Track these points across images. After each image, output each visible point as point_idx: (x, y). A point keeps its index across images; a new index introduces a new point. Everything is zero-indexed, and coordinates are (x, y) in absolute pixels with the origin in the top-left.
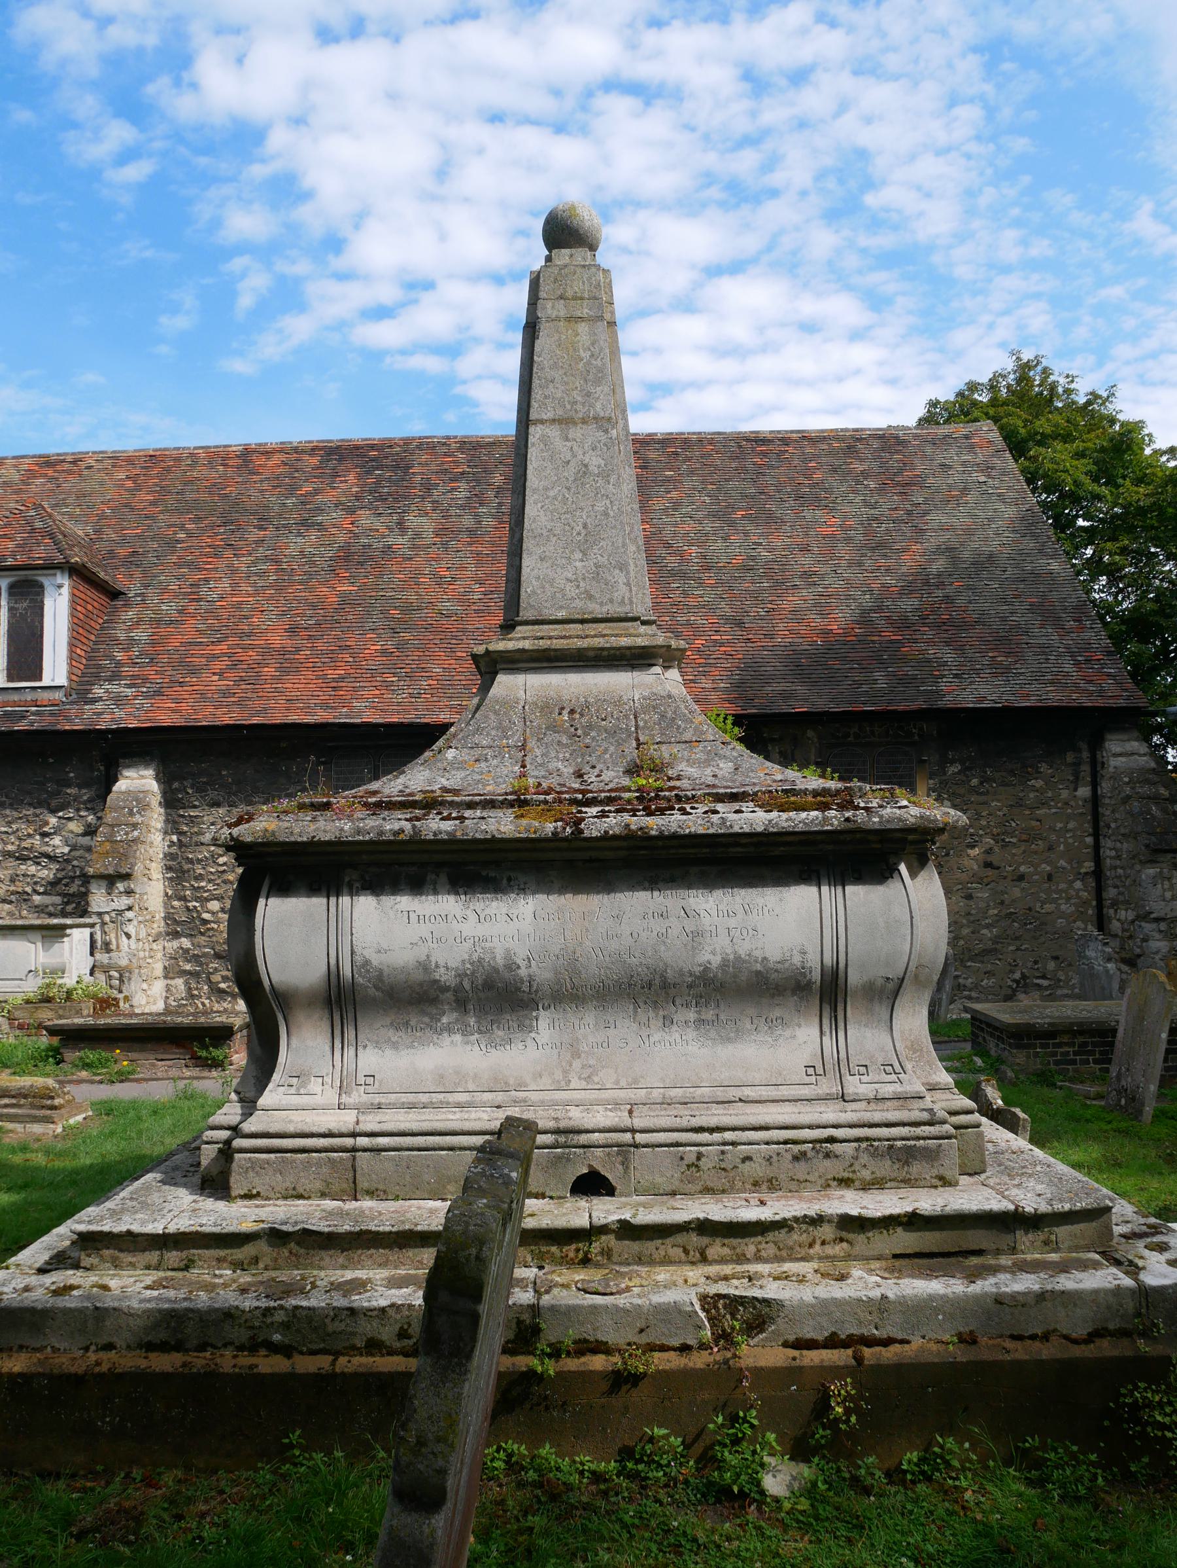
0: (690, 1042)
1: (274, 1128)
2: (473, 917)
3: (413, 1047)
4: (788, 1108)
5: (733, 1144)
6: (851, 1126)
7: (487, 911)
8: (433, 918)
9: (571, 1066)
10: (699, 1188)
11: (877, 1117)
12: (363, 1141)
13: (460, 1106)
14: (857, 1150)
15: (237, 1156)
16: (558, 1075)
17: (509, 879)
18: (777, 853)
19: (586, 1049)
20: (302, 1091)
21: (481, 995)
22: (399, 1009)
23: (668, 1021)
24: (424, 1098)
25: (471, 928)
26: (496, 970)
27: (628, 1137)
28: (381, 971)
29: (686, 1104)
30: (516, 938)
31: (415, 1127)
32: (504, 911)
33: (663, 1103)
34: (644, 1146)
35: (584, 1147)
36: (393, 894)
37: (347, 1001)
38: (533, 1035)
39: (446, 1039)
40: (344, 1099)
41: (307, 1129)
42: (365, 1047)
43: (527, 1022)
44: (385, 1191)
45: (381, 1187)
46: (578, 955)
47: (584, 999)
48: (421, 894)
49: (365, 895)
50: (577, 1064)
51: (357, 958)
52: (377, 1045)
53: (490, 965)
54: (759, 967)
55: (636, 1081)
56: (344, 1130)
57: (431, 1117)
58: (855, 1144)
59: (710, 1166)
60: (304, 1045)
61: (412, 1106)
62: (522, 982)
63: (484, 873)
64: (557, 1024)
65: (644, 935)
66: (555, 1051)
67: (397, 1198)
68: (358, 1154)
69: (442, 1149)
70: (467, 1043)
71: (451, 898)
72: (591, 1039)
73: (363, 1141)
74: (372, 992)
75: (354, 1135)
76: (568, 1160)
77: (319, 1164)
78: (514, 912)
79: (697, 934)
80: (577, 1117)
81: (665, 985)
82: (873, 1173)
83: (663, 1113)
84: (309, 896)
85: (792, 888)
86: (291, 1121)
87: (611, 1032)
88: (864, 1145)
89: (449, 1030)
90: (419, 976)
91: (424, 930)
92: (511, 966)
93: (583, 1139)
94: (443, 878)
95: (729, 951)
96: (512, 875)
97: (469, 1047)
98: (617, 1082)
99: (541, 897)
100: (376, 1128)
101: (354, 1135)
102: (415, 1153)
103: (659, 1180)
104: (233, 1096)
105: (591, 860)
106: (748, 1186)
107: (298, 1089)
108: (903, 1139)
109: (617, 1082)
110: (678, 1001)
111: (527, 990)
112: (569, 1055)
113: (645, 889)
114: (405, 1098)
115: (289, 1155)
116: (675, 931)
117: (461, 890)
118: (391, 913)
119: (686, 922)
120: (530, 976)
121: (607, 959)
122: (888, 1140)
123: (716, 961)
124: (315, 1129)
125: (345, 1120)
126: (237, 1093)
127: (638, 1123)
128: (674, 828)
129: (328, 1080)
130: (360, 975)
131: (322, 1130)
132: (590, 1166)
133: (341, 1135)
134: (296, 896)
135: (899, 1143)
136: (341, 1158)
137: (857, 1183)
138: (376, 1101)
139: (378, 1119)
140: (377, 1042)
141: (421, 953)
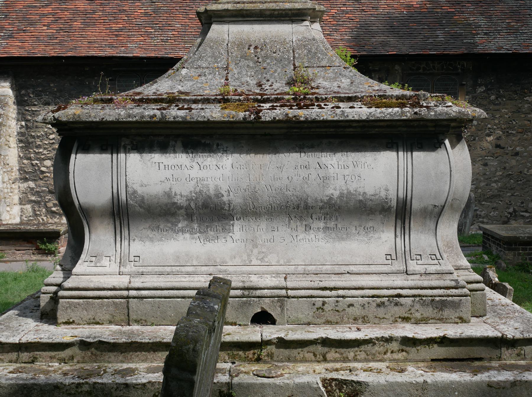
0: (320, 240)
1: (81, 285)
2: (196, 167)
3: (161, 240)
4: (375, 277)
5: (343, 297)
6: (411, 288)
7: (205, 163)
8: (173, 167)
9: (252, 252)
10: (323, 321)
11: (426, 284)
12: (133, 293)
13: (189, 274)
14: (413, 301)
15: (61, 300)
16: (245, 257)
17: (218, 145)
18: (373, 132)
19: (261, 243)
20: (98, 265)
21: (201, 211)
22: (154, 219)
23: (308, 228)
24: (168, 269)
25: (195, 173)
26: (210, 197)
27: (283, 292)
28: (143, 197)
29: (317, 274)
30: (221, 179)
31: (163, 285)
32: (215, 163)
33: (304, 274)
34: (292, 298)
35: (259, 297)
36: (150, 153)
37: (123, 214)
38: (231, 234)
39: (181, 236)
40: (122, 269)
41: (101, 286)
42: (134, 240)
43: (227, 227)
44: (146, 321)
45: (143, 318)
46: (257, 189)
47: (260, 214)
48: (166, 153)
49: (134, 153)
50: (255, 251)
51: (129, 189)
52: (141, 239)
53: (206, 194)
54: (361, 198)
55: (289, 261)
56: (122, 286)
57: (172, 280)
58: (413, 299)
59: (330, 308)
60: (99, 238)
61: (161, 274)
62: (225, 204)
63: (203, 141)
64: (244, 228)
65: (295, 178)
66: (243, 244)
67: (152, 324)
68: (130, 300)
69: (178, 297)
70: (193, 238)
71: (184, 156)
72: (264, 237)
73: (133, 293)
74: (138, 209)
75: (128, 289)
76: (250, 304)
77: (108, 305)
78: (220, 164)
79: (326, 179)
80: (255, 280)
81: (307, 207)
82: (422, 314)
83: (304, 279)
84: (101, 153)
85: (382, 153)
86: (92, 281)
87: (275, 233)
88: (417, 299)
89: (183, 231)
90: (165, 200)
91: (168, 173)
92: (219, 195)
93: (258, 293)
94: (179, 144)
95: (344, 188)
96: (220, 142)
97: (194, 241)
98: (278, 262)
99: (236, 156)
100: (141, 285)
101: (128, 289)
102: (163, 299)
103: (300, 316)
104: (58, 267)
105: (265, 135)
106: (351, 320)
107: (96, 263)
108: (440, 296)
109: (278, 262)
110: (314, 216)
111: (227, 209)
112: (251, 247)
113: (296, 152)
114: (157, 269)
115: (91, 300)
116: (313, 176)
117: (189, 151)
118: (149, 164)
119: (320, 171)
120: (229, 201)
121: (274, 191)
122: (431, 296)
123: (336, 194)
124: (105, 286)
125: (123, 281)
126: (61, 265)
127: (290, 284)
128: (314, 116)
129: (113, 258)
130: (131, 199)
131: (110, 286)
132: (262, 308)
133: (121, 289)
134: (93, 153)
135: (437, 299)
136: (121, 302)
137: (413, 320)
138: (141, 270)
139: (142, 280)
140: (141, 238)
141: (166, 187)
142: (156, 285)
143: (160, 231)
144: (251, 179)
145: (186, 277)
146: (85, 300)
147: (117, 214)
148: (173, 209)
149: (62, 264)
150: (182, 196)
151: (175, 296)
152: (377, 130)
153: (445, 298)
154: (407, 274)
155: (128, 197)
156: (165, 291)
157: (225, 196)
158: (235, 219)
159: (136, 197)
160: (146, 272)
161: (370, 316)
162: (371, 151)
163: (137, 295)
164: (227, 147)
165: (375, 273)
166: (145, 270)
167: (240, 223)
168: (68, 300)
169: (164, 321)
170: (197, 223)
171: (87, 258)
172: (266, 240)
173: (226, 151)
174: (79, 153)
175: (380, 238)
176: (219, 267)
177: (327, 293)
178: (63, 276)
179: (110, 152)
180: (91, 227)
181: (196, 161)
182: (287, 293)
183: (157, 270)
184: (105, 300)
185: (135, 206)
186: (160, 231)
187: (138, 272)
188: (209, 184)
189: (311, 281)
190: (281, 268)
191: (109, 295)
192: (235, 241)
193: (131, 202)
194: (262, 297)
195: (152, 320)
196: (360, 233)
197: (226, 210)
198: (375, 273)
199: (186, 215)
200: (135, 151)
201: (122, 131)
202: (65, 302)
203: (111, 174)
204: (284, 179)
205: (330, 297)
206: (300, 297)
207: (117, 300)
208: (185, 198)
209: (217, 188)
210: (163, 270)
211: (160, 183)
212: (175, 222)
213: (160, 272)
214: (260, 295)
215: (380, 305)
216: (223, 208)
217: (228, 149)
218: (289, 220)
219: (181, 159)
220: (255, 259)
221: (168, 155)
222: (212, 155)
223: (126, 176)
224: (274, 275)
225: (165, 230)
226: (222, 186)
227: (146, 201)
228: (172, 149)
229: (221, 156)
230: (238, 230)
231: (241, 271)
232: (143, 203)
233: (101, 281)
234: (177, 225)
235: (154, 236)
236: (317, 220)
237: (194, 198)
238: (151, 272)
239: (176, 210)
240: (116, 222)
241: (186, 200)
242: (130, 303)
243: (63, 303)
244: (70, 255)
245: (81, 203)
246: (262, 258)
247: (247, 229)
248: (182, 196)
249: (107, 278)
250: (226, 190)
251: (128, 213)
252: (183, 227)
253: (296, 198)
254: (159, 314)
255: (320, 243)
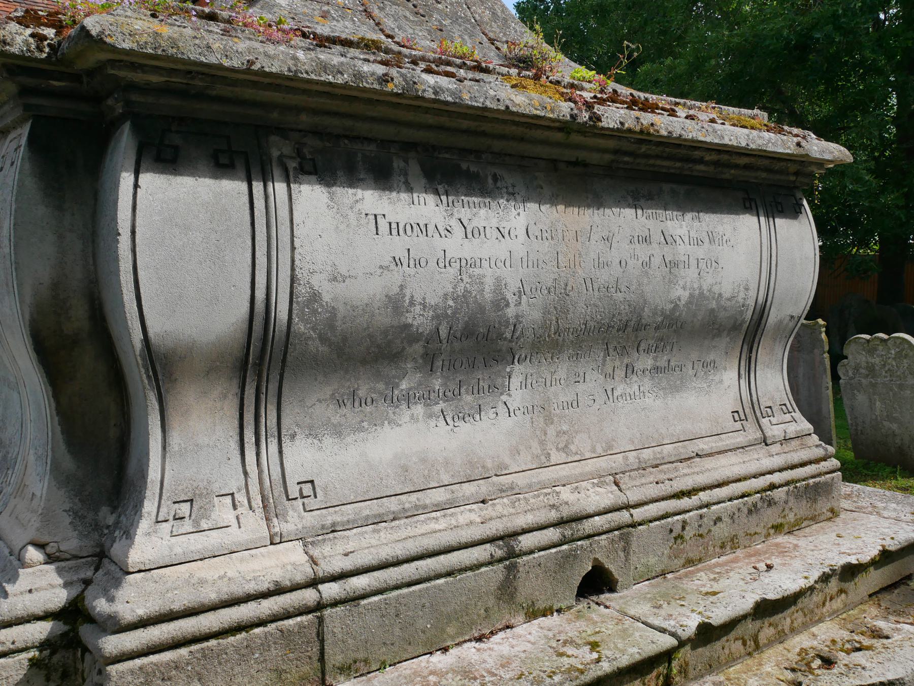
0: (647, 394)
1: (180, 600)
2: (458, 230)
3: (361, 429)
4: (732, 458)
5: (707, 505)
6: (780, 470)
7: (475, 223)
8: (408, 228)
9: (546, 434)
10: (682, 561)
11: (796, 458)
12: (330, 590)
13: (439, 508)
14: (787, 493)
15: (113, 669)
16: (536, 449)
17: (495, 178)
18: (727, 176)
19: (558, 411)
20: (204, 525)
21: (457, 345)
22: (347, 372)
23: (630, 370)
24: (392, 505)
25: (456, 246)
26: (481, 309)
27: (624, 517)
28: (333, 312)
29: (657, 466)
30: (508, 264)
31: (400, 551)
32: (494, 223)
33: (639, 468)
34: (640, 524)
35: (589, 537)
36: (351, 186)
37: (272, 362)
38: (504, 398)
39: (405, 414)
40: (278, 526)
41: (239, 590)
42: (293, 437)
43: (499, 381)
44: (366, 661)
45: (361, 655)
46: (569, 288)
47: (563, 345)
48: (390, 189)
49: (309, 183)
50: (551, 431)
51: (301, 290)
52: (312, 433)
53: (476, 302)
54: (714, 305)
55: (610, 447)
56: (299, 578)
57: (410, 532)
58: (785, 488)
59: (691, 534)
60: (189, 443)
61: (378, 520)
62: (507, 322)
63: (464, 166)
64: (529, 381)
65: (631, 263)
66: (528, 417)
67: (383, 666)
68: (327, 612)
69: (438, 576)
70: (430, 416)
71: (431, 199)
72: (562, 398)
73: (330, 590)
74: (315, 346)
75: (314, 583)
76: (575, 556)
77: (265, 645)
78: (506, 226)
79: (672, 265)
80: (576, 499)
81: (640, 327)
82: (795, 515)
83: (643, 481)
84: (215, 177)
85: (741, 216)
86: (202, 582)
87: (581, 387)
88: (791, 488)
89: (409, 399)
90: (384, 319)
91: (398, 245)
92: (500, 303)
93: (588, 526)
94: (414, 168)
95: (696, 286)
96: (499, 172)
97: (432, 423)
98: (593, 450)
99: (532, 206)
100: (347, 564)
101: (314, 583)
102: (405, 591)
103: (652, 560)
104: (33, 554)
105: (576, 163)
106: (717, 550)
107: (196, 523)
108: (813, 477)
109: (593, 450)
110: (643, 346)
111: (508, 335)
112: (542, 424)
113: (629, 206)
114: (369, 509)
115: (213, 643)
116: (657, 261)
117: (441, 188)
118: (352, 216)
119: (666, 249)
120: (517, 316)
121: (596, 293)
122: (804, 480)
123: (685, 295)
124: (251, 588)
125: (289, 562)
126: (40, 546)
127: (633, 496)
128: (677, 132)
129: (241, 498)
130: (302, 320)
131: (264, 586)
132: (596, 560)
133: (278, 590)
134: (192, 175)
135: (811, 481)
136: (301, 626)
137: (786, 529)
138: (329, 521)
139: (340, 548)
140: (311, 428)
141: (394, 279)
142: (385, 553)
143: (357, 404)
144: (561, 264)
145: (437, 519)
146: (194, 647)
147: (255, 364)
148: (398, 341)
149: (44, 539)
150: (425, 307)
151: (433, 574)
152: (733, 171)
153: (818, 479)
154: (767, 445)
155: (295, 312)
156: (406, 566)
157: (512, 305)
158: (516, 361)
159: (315, 312)
160: (343, 524)
161: (741, 534)
162: (728, 213)
163: (343, 595)
164: (514, 186)
165: (730, 450)
166: (338, 519)
167: (523, 370)
168: (138, 662)
169: (410, 648)
170: (442, 376)
171: (163, 510)
172: (565, 404)
173: (513, 194)
174: (147, 171)
175: (721, 381)
176: (495, 479)
177: (685, 502)
178: (60, 581)
179: (243, 174)
180: (170, 412)
181: (456, 216)
182: (632, 515)
183: (367, 512)
184: (257, 631)
185: (310, 338)
186: (357, 404)
187: (323, 527)
188: (484, 276)
189: (657, 483)
190: (603, 464)
191: (268, 612)
192: (512, 414)
193: (300, 326)
194: (594, 535)
195: (382, 653)
196: (698, 374)
197: (505, 339)
198: (730, 450)
199: (422, 356)
200: (313, 178)
201: (275, 115)
202: (132, 672)
203: (249, 243)
204: (614, 264)
205: (688, 511)
206: (651, 521)
207: (291, 622)
208: (431, 313)
209: (499, 284)
210: (382, 511)
211: (379, 271)
212: (394, 377)
213: (375, 516)
214: (591, 532)
215: (753, 510)
216: (500, 336)
217: (516, 189)
218: (605, 357)
219: (423, 208)
220: (554, 450)
221: (394, 194)
222: (487, 200)
223: (293, 249)
224: (595, 481)
225: (369, 400)
226: (509, 280)
227: (338, 323)
228: (402, 179)
229: (506, 208)
230: (520, 386)
231: (539, 483)
232: (332, 327)
233: (230, 574)
234: (398, 385)
235: (343, 420)
236: (645, 354)
237: (449, 312)
238: (354, 521)
239: (405, 344)
240: (247, 388)
241: (433, 318)
242: (327, 621)
243: (122, 675)
244: (67, 506)
245: (151, 333)
246: (566, 446)
247: (534, 382)
248: (425, 307)
249: (242, 560)
250: (516, 290)
251: (284, 361)
252: (410, 389)
253: (627, 307)
254: (397, 631)
255: (647, 399)
